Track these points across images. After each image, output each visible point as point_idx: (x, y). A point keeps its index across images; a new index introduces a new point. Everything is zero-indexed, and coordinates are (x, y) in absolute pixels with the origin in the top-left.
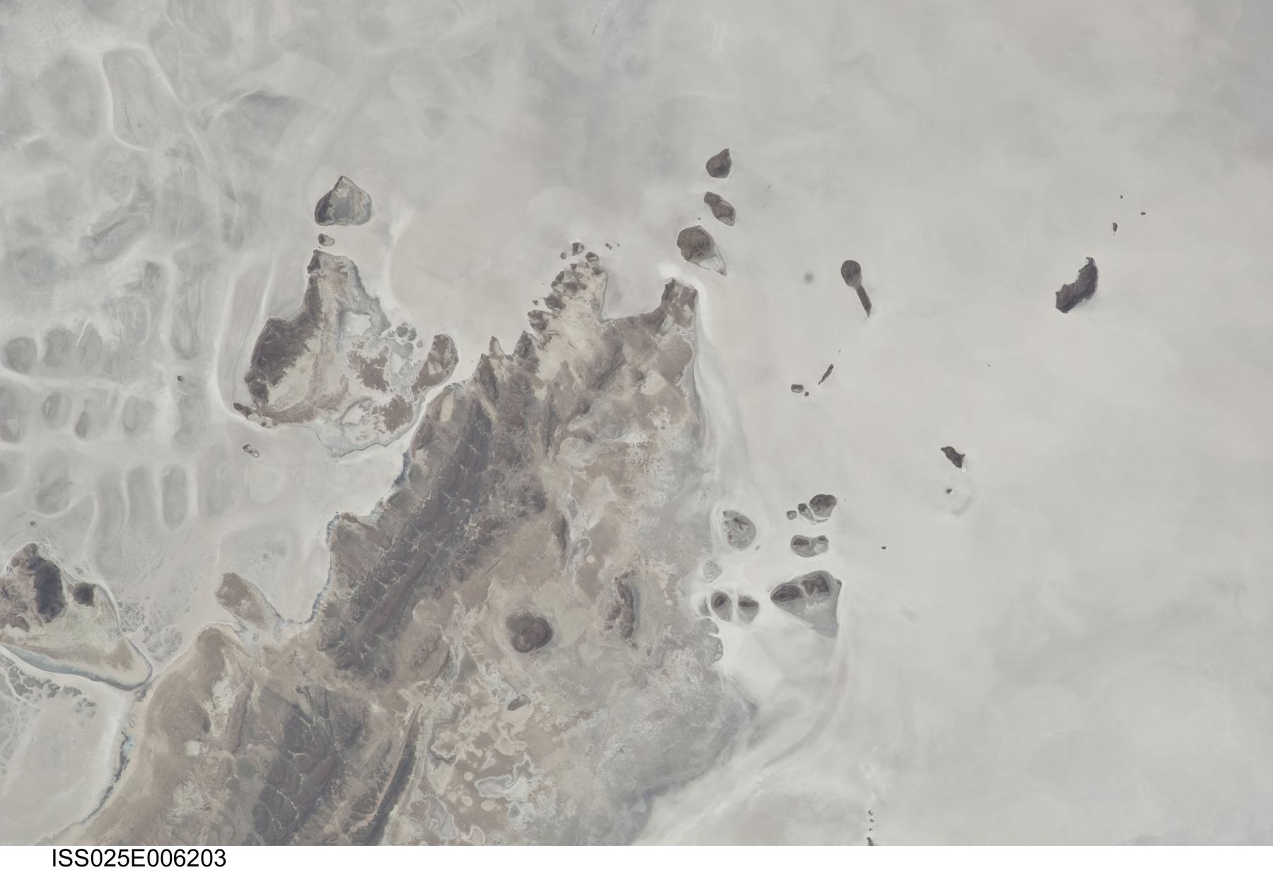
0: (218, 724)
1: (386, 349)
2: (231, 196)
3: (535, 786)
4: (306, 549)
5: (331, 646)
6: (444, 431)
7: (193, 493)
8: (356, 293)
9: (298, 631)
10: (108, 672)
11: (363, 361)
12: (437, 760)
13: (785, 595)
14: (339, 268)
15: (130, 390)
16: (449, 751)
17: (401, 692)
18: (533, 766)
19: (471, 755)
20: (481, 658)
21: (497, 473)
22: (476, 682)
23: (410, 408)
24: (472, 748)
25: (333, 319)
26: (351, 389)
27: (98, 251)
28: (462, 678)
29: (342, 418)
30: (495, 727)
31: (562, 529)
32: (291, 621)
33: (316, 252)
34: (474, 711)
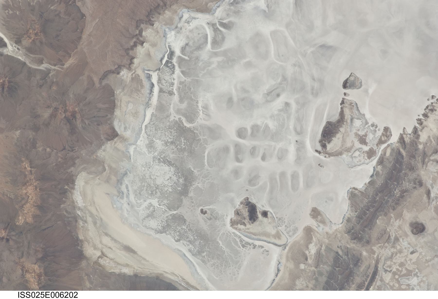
0: (311, 258)
1: (367, 131)
2: (314, 79)
4: (340, 199)
5: (349, 232)
6: (387, 159)
7: (301, 180)
8: (357, 112)
9: (338, 227)
10: (273, 240)
11: (359, 135)
12: (386, 271)
14: (351, 104)
15: (280, 145)
16: (390, 268)
17: (373, 248)
19: (397, 270)
20: (401, 237)
21: (406, 173)
22: (399, 245)
23: (375, 152)
24: (398, 267)
25: (349, 121)
26: (355, 145)
27: (269, 98)
28: (394, 243)
29: (352, 155)
32: (335, 224)
33: (343, 98)
34: (398, 255)
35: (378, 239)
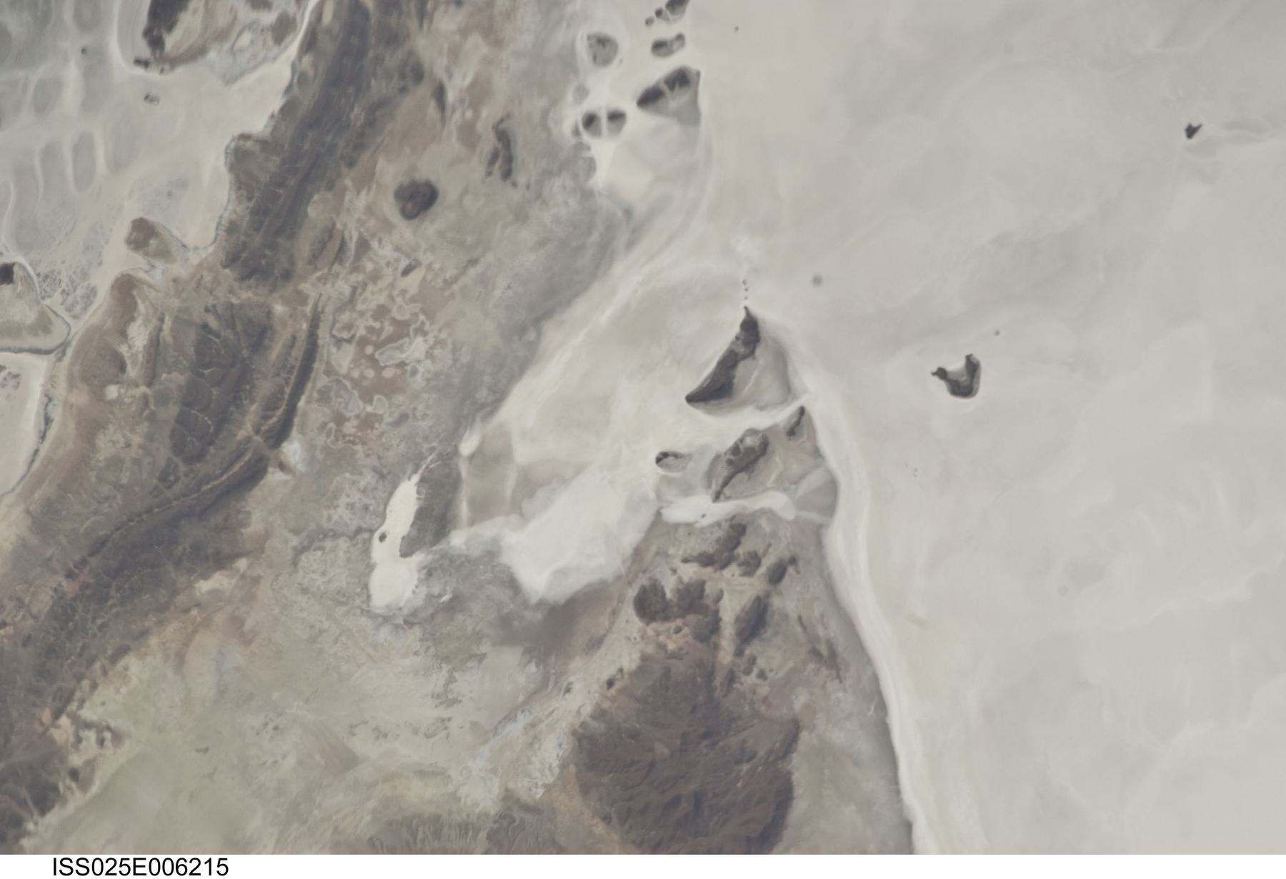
0: (134, 363)
3: (431, 341)
12: (339, 342)
13: (649, 98)
18: (428, 323)
19: (370, 330)
20: (373, 235)
22: (371, 259)
24: (371, 323)
28: (358, 257)
30: (391, 297)
31: (440, 93)
32: (196, 248)
34: (370, 287)
35: (314, 259)
